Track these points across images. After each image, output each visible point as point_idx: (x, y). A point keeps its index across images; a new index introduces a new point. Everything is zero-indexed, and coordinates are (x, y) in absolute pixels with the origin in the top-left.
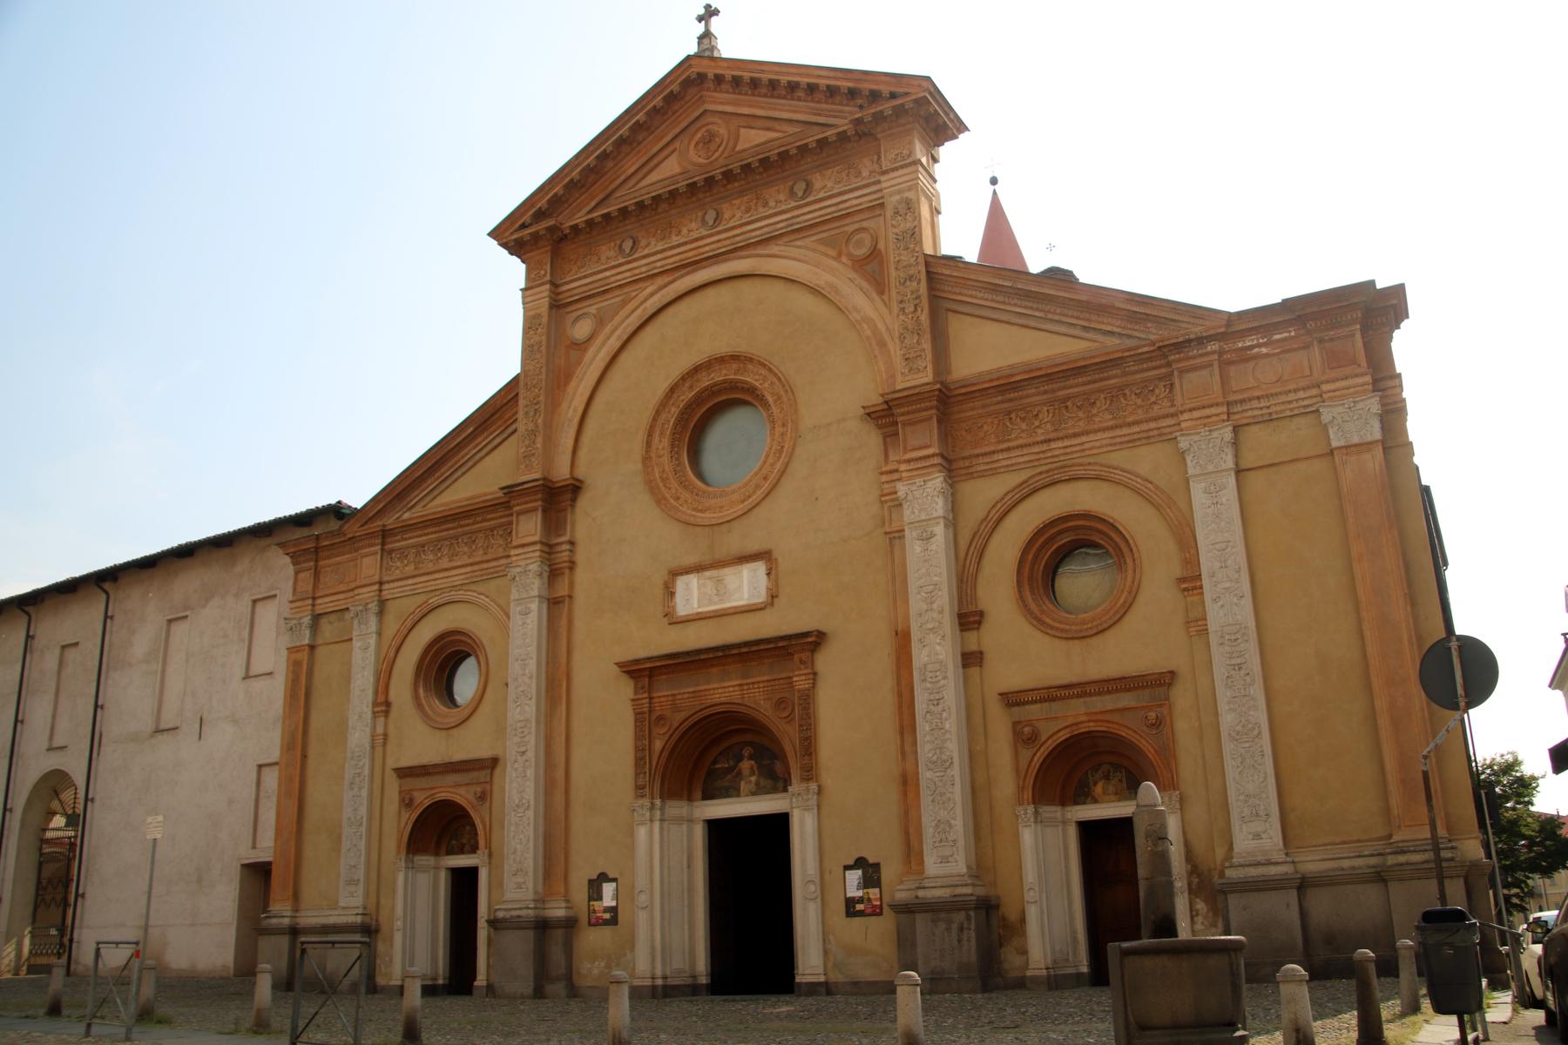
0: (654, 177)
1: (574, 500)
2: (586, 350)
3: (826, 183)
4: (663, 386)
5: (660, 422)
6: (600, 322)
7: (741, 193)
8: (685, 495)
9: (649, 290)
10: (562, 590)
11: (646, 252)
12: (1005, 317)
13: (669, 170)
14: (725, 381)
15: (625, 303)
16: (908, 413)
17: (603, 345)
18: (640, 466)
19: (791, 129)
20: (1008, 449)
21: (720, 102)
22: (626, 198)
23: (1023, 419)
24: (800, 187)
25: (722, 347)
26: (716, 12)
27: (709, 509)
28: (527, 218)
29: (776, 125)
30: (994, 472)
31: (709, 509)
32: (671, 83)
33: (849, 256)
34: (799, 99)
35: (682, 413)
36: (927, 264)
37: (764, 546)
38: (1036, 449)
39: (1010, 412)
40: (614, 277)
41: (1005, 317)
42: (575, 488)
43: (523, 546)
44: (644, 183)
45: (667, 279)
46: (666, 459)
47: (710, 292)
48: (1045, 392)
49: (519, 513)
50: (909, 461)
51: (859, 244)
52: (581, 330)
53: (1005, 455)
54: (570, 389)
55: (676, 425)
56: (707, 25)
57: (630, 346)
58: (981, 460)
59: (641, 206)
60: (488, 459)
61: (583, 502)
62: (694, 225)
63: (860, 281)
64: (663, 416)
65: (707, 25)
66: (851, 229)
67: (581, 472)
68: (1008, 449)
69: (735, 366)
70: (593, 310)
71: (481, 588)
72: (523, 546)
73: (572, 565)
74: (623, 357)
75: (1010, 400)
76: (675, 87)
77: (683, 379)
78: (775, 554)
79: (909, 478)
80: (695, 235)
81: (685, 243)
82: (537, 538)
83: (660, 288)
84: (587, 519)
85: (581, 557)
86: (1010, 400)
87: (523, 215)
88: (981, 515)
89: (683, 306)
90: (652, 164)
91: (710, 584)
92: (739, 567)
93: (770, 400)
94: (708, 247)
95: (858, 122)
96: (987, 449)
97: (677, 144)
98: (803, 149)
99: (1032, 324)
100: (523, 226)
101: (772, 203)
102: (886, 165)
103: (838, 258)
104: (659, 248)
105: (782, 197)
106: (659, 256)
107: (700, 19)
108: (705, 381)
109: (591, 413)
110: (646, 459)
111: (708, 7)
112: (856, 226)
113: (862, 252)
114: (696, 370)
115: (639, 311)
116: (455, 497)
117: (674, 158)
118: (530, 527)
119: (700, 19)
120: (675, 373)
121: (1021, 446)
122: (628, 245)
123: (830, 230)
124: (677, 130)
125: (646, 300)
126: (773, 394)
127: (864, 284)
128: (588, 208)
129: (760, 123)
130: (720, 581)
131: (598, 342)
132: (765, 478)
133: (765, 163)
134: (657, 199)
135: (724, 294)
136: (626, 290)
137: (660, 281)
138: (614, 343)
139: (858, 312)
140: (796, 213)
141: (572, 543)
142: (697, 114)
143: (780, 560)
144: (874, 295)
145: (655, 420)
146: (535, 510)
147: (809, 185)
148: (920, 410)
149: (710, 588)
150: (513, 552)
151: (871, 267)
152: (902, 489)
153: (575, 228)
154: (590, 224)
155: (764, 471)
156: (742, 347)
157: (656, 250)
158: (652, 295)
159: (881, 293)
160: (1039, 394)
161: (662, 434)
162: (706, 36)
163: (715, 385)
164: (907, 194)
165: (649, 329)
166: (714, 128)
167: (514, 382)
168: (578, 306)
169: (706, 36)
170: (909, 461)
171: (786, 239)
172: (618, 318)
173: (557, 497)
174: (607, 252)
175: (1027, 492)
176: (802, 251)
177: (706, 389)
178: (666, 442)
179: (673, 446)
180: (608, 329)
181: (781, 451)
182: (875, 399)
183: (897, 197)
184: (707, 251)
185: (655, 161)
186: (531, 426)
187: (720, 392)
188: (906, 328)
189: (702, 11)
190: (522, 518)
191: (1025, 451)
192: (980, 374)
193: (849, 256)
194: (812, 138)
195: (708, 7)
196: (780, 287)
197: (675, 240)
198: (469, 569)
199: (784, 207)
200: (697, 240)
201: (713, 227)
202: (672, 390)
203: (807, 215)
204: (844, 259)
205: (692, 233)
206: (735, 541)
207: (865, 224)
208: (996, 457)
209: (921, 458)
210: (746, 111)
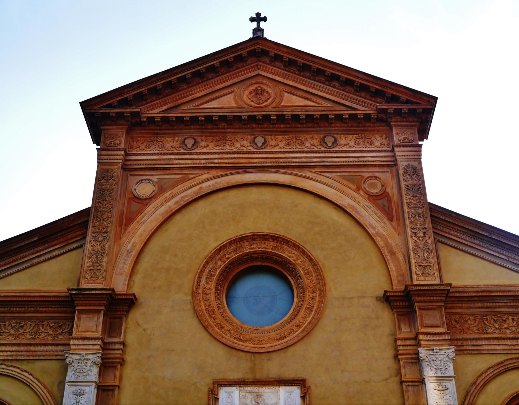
0: (214, 104)
1: (128, 312)
2: (146, 205)
3: (347, 141)
4: (213, 245)
5: (207, 270)
6: (161, 189)
7: (284, 132)
8: (227, 326)
9: (205, 176)
10: (110, 381)
11: (204, 150)
12: (480, 254)
13: (226, 103)
14: (263, 252)
15: (183, 180)
16: (425, 301)
17: (163, 204)
18: (189, 298)
19: (324, 103)
20: (489, 339)
21: (271, 72)
22: (186, 111)
23: (496, 321)
24: (329, 140)
25: (264, 228)
26: (265, 19)
27: (250, 340)
28: (115, 101)
29: (314, 98)
30: (479, 353)
31: (250, 340)
32: (242, 49)
33: (366, 193)
34: (334, 87)
35: (226, 267)
36: (430, 209)
37: (300, 375)
38: (509, 342)
39: (486, 315)
40: (176, 160)
41: (480, 254)
42: (129, 302)
43: (84, 338)
44: (205, 106)
45: (220, 173)
46: (212, 296)
47: (254, 190)
48: (511, 307)
49: (81, 312)
50: (426, 334)
51: (373, 185)
52: (144, 190)
53: (486, 342)
54: (130, 228)
55: (221, 274)
56: (258, 25)
57: (184, 211)
58: (469, 343)
59: (209, 119)
60: (45, 265)
61: (136, 316)
62: (245, 143)
63: (373, 208)
64: (210, 266)
65: (258, 25)
66: (366, 175)
67: (136, 290)
68: (489, 339)
69: (272, 244)
70: (155, 178)
71: (24, 367)
72: (84, 338)
73: (122, 362)
74: (178, 217)
75: (487, 307)
76: (244, 53)
77: (231, 243)
78: (308, 384)
79: (427, 345)
80: (245, 150)
81: (234, 153)
82: (98, 334)
83: (215, 178)
84: (135, 328)
85: (129, 358)
86: (487, 307)
87: (112, 98)
88: (471, 380)
89: (232, 194)
90: (214, 96)
91: (250, 397)
92: (277, 388)
93: (302, 272)
94: (257, 159)
95: (384, 111)
96: (472, 336)
97: (235, 89)
98: (339, 117)
99: (498, 261)
100: (110, 106)
101: (308, 144)
102: (396, 142)
103: (358, 190)
104: (214, 151)
105: (315, 142)
106: (217, 156)
107: (252, 20)
108: (247, 248)
109: (147, 250)
110: (194, 294)
111: (258, 14)
112: (370, 174)
113: (375, 191)
114: (242, 239)
115: (197, 188)
116: (6, 288)
117: (231, 96)
118: (90, 325)
119: (252, 20)
120: (224, 238)
121: (496, 339)
122: (190, 142)
123: (353, 173)
124: (236, 80)
125: (202, 182)
126: (304, 269)
127: (379, 213)
128: (160, 110)
129: (300, 93)
130: (259, 396)
131: (159, 201)
132: (298, 326)
133: (296, 118)
134: (223, 119)
135: (266, 193)
136: (185, 172)
137: (214, 173)
138: (172, 205)
139: (374, 228)
140: (327, 155)
141: (123, 344)
142: (252, 74)
143: (313, 387)
144: (385, 220)
145: (204, 267)
146: (98, 312)
147: (335, 142)
148: (433, 301)
149: (250, 399)
150: (72, 342)
151: (381, 200)
152: (423, 352)
153: (151, 120)
154: (165, 120)
155: (227, 326)
156: (281, 232)
157: (209, 150)
158: (207, 180)
159: (391, 220)
160: (508, 307)
161: (209, 279)
162: (258, 31)
163: (255, 253)
164: (412, 163)
165: (202, 203)
166: (264, 87)
167: (85, 213)
168: (142, 173)
169: (258, 31)
170: (426, 334)
171: (317, 170)
172: (176, 190)
173: (118, 307)
174: (171, 143)
175: (502, 369)
176: (330, 180)
177: (248, 254)
178: (212, 285)
179: (216, 289)
180: (168, 194)
181: (311, 310)
182: (399, 287)
183: (406, 163)
184: (256, 162)
185: (217, 95)
186: (98, 248)
187: (256, 259)
188: (417, 246)
189: (254, 16)
190: (83, 316)
191: (501, 342)
192: (472, 286)
193: (366, 193)
194: (346, 113)
195: (258, 14)
196: (309, 200)
197: (228, 149)
198: (15, 348)
199: (316, 149)
200: (249, 153)
201: (260, 148)
202: (220, 249)
203: (334, 158)
204: (362, 193)
205: (241, 146)
206: (273, 368)
207: (376, 174)
208: (480, 343)
209: (435, 334)
210: (290, 83)
